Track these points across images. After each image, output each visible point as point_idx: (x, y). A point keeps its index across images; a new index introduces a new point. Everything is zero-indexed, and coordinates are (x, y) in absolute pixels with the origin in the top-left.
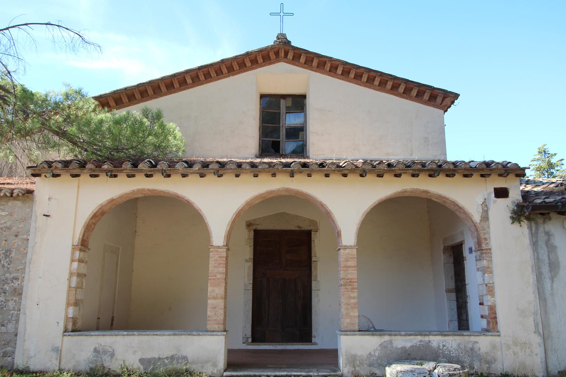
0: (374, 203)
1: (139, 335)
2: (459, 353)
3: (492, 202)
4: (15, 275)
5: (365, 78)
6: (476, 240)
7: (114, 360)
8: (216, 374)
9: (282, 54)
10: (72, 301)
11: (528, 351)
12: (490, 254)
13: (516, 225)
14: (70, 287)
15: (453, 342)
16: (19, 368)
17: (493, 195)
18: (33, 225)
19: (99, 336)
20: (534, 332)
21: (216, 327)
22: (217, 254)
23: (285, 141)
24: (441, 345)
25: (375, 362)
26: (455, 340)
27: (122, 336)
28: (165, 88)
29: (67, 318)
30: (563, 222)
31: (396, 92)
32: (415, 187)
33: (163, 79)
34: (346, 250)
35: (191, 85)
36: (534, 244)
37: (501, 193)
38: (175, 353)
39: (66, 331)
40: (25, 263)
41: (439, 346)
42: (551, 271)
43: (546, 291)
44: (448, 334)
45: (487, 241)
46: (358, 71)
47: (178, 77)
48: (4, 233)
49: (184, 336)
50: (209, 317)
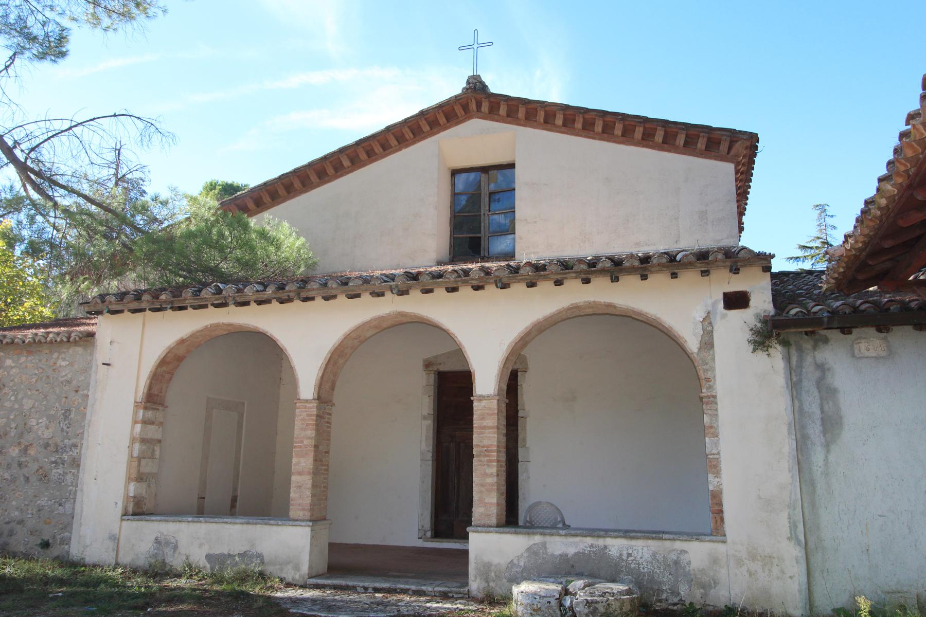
0: (526, 328)
1: (206, 522)
2: (653, 569)
3: (718, 318)
4: (74, 441)
5: (599, 127)
7: (176, 555)
8: (298, 581)
9: (473, 106)
10: (134, 476)
11: (776, 570)
12: (714, 405)
13: (761, 355)
14: (132, 457)
15: (645, 549)
16: (74, 559)
17: (721, 305)
19: (161, 522)
20: (789, 539)
21: (300, 514)
22: (304, 412)
23: (489, 237)
24: (625, 553)
25: (518, 576)
26: (647, 546)
27: (187, 523)
28: (316, 177)
29: (127, 497)
30: (852, 346)
31: (651, 143)
32: (592, 300)
33: (311, 165)
34: (482, 402)
35: (350, 168)
36: (795, 386)
37: (737, 301)
38: (249, 549)
40: (84, 426)
41: (621, 555)
42: (825, 432)
43: (815, 468)
44: (636, 536)
45: (710, 383)
46: (587, 116)
47: (332, 159)
48: (64, 388)
49: (260, 525)
50: (292, 500)
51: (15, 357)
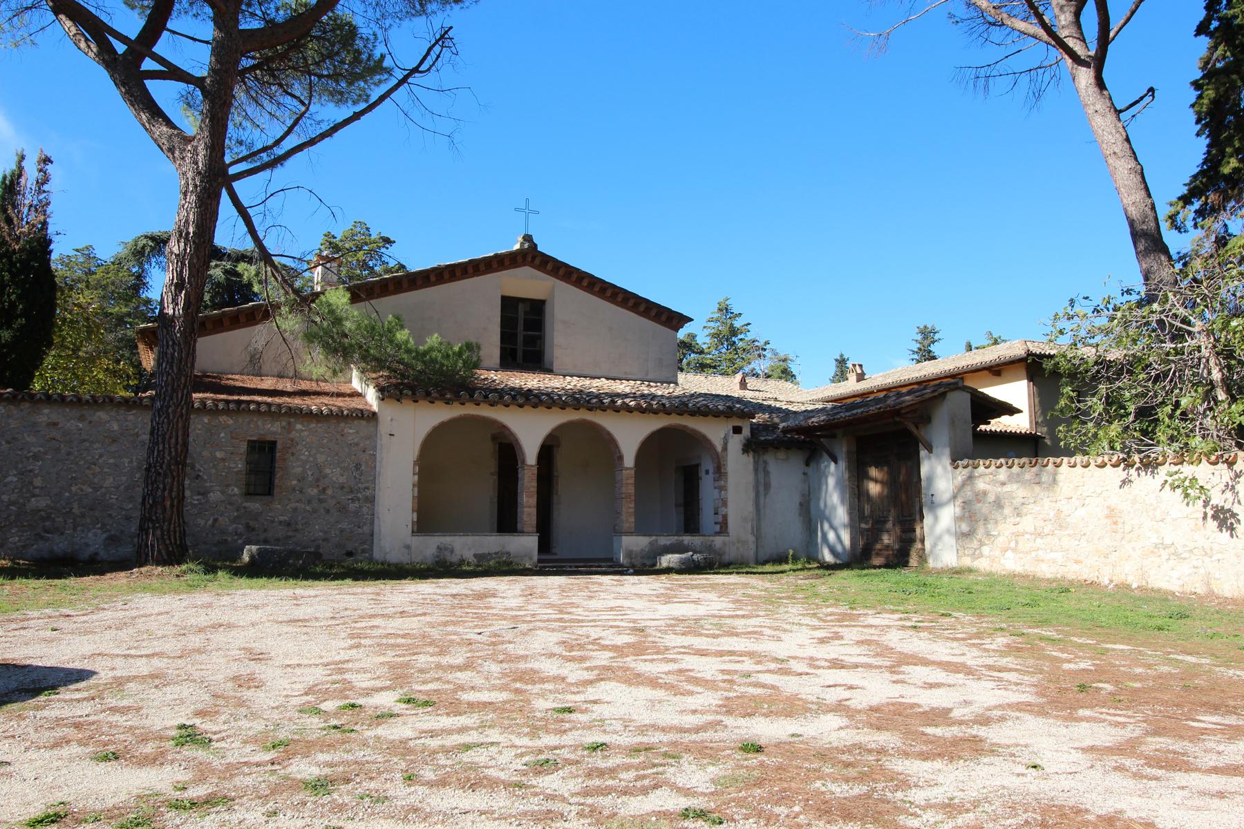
4: (367, 485)
6: (716, 465)
13: (746, 455)
18: (379, 442)
36: (756, 470)
37: (737, 430)
39: (413, 532)
51: (306, 423)
